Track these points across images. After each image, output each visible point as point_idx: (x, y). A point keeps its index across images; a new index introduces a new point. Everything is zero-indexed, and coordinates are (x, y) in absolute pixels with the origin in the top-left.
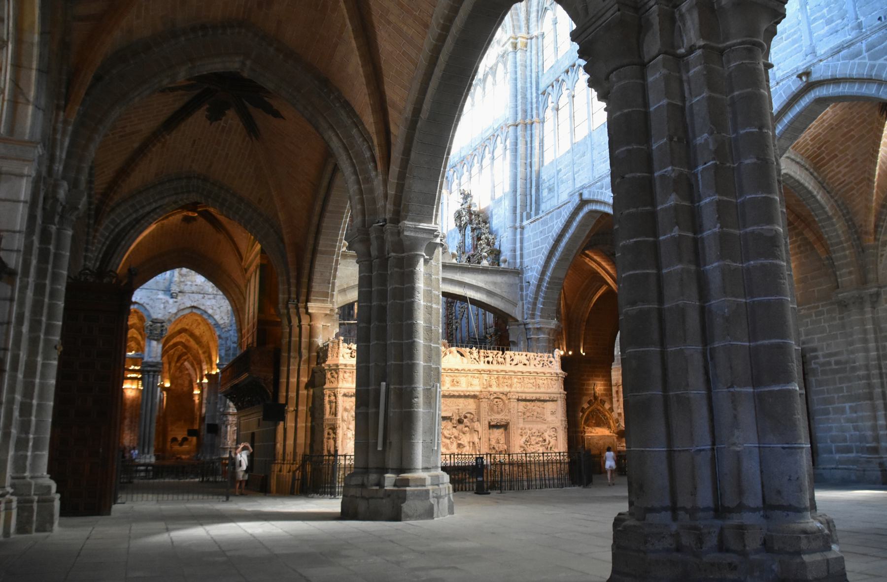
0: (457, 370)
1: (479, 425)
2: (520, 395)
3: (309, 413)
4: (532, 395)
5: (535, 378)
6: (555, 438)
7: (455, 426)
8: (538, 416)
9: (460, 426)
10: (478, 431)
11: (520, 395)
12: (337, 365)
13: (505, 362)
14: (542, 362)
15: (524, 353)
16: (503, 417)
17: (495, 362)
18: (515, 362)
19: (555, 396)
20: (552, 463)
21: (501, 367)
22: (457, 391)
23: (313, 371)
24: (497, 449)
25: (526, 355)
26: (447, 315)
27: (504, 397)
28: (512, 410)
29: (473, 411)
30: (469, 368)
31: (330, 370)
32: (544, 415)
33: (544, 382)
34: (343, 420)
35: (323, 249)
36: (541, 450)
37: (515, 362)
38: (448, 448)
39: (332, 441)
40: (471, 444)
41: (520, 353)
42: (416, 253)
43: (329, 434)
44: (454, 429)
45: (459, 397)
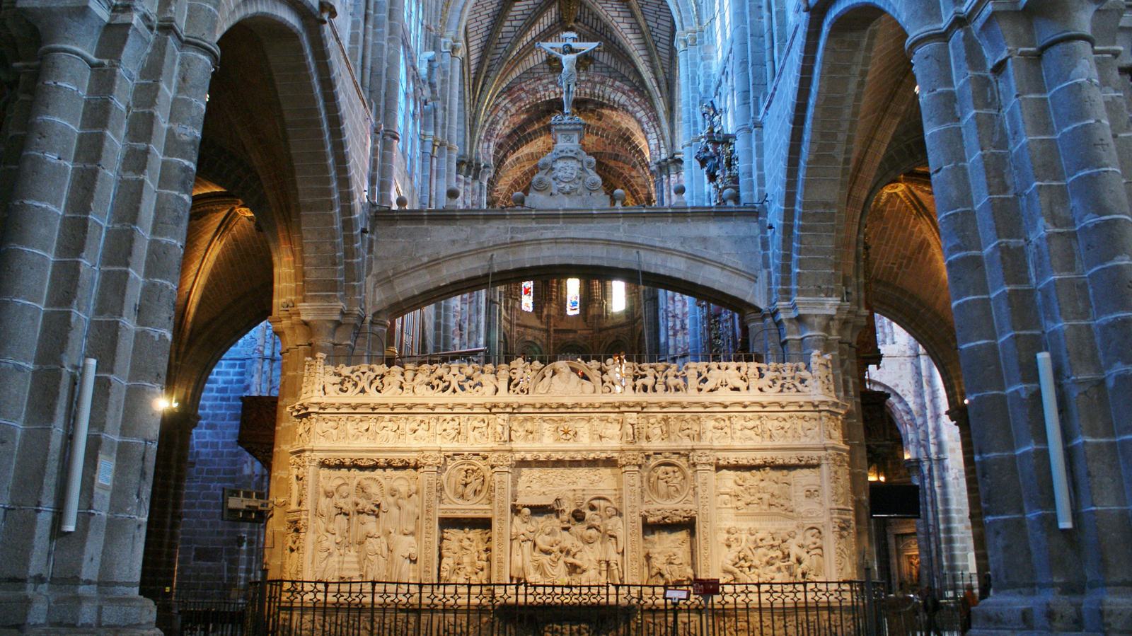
0: (563, 405)
1: (620, 524)
2: (720, 455)
4: (752, 455)
5: (760, 417)
6: (818, 551)
7: (567, 525)
8: (774, 501)
9: (578, 528)
10: (615, 537)
11: (720, 455)
13: (686, 386)
14: (779, 383)
15: (733, 365)
16: (678, 506)
17: (660, 387)
18: (710, 385)
19: (815, 454)
20: (760, 609)
21: (672, 396)
24: (667, 576)
25: (739, 369)
26: (710, 340)
27: (682, 462)
28: (699, 490)
30: (590, 401)
32: (789, 499)
33: (782, 424)
35: (308, 200)
36: (779, 578)
37: (710, 385)
38: (544, 574)
40: (604, 566)
41: (723, 364)
42: (53, 46)
44: (565, 533)
45: (574, 463)
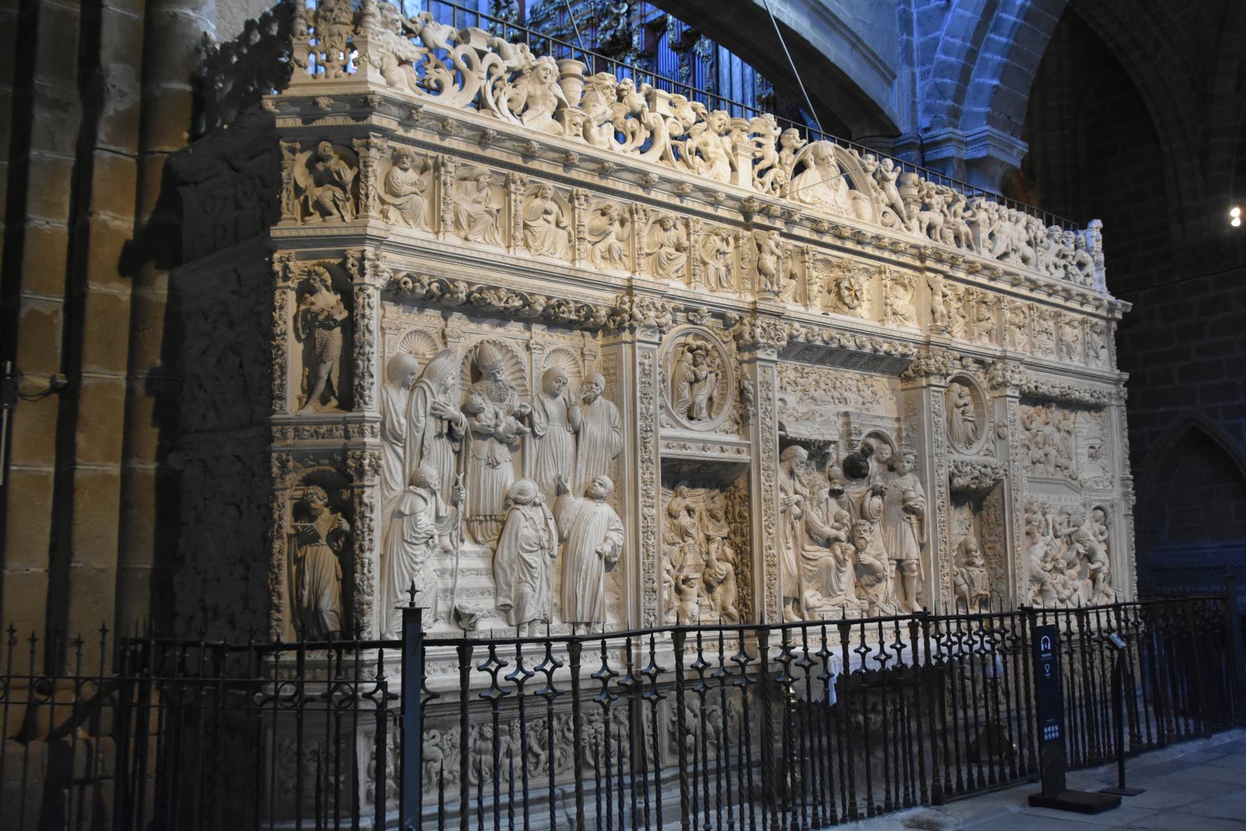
1: (919, 486)
3: (147, 406)
7: (838, 487)
9: (854, 490)
12: (362, 104)
22: (854, 332)
23: (169, 171)
29: (888, 427)
31: (310, 140)
34: (389, 435)
38: (828, 591)
39: (325, 559)
43: (303, 511)
44: (833, 502)
